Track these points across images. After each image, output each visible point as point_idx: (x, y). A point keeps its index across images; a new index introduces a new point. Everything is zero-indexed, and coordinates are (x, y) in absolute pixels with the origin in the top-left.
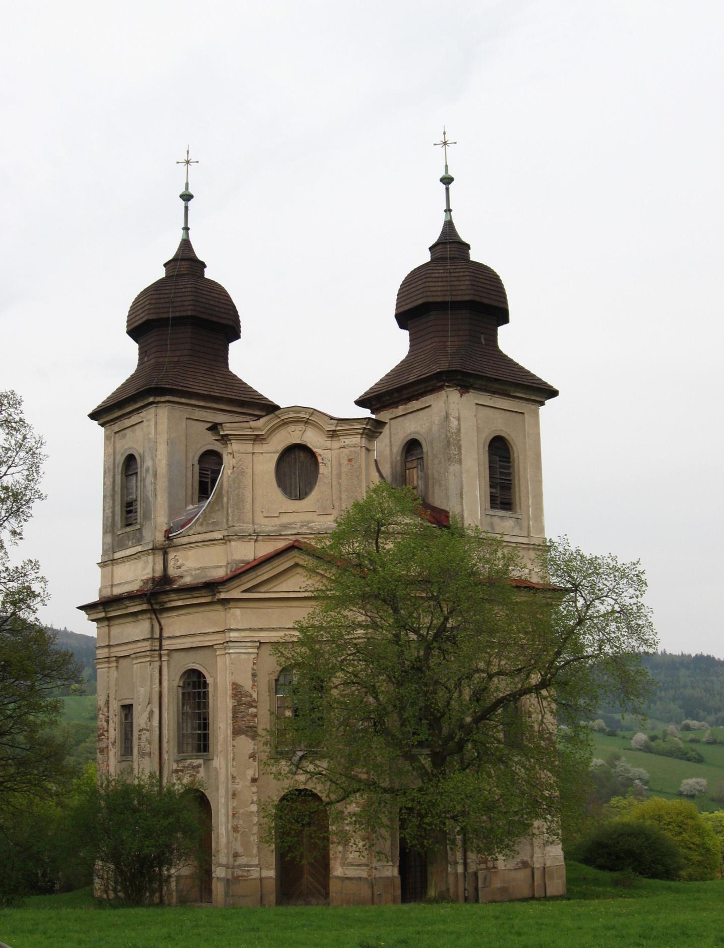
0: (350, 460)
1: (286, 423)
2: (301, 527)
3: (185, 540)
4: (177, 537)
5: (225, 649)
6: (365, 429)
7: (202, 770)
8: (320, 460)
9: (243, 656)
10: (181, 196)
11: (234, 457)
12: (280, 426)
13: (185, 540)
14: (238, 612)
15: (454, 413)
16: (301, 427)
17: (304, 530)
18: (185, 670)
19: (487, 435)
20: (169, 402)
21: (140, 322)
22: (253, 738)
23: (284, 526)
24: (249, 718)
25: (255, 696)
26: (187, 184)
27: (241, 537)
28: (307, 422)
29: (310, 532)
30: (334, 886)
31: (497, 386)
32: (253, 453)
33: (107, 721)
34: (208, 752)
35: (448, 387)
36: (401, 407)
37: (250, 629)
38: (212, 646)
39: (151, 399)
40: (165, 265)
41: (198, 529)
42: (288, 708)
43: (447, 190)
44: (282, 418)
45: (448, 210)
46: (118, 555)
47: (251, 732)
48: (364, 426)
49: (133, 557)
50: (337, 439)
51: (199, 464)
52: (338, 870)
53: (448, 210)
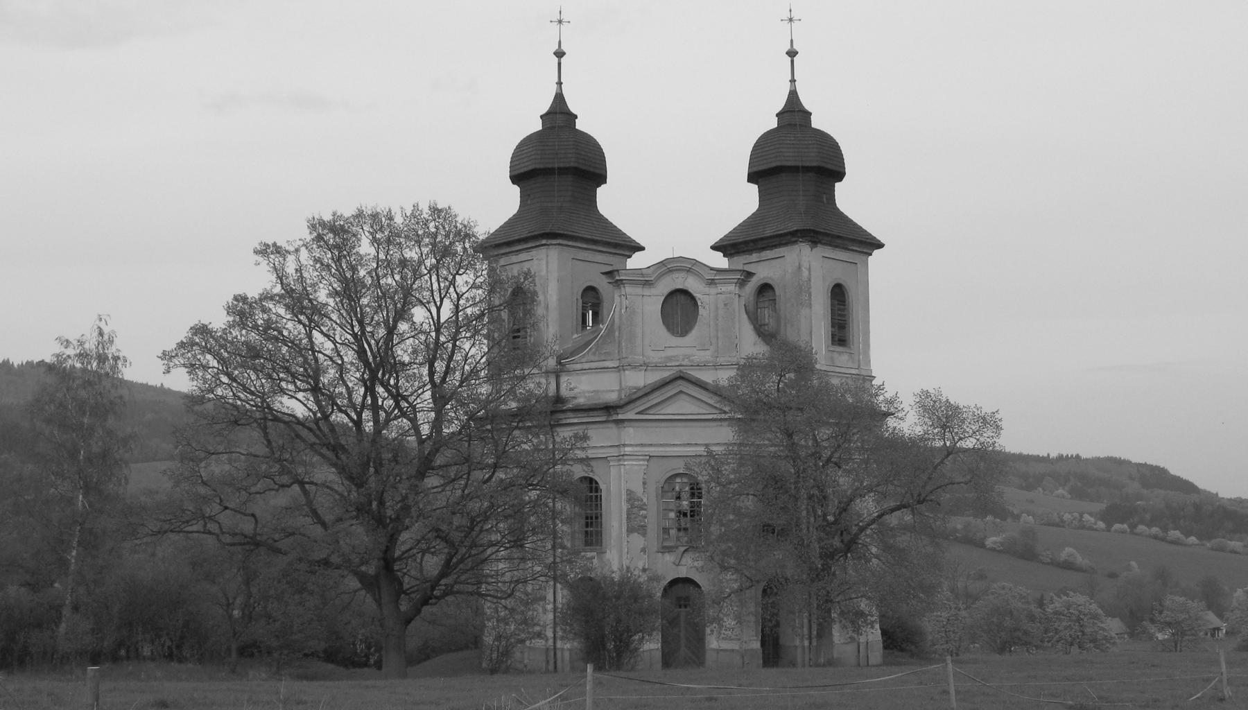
0: (725, 305)
1: (671, 271)
2: (683, 360)
3: (578, 366)
4: (569, 363)
5: (620, 460)
6: (739, 279)
7: (595, 561)
8: (699, 304)
9: (636, 468)
10: (555, 53)
11: (626, 299)
12: (668, 272)
13: (578, 366)
14: (631, 430)
15: (805, 265)
16: (683, 274)
17: (686, 362)
19: (830, 283)
20: (559, 244)
22: (644, 535)
23: (670, 358)
24: (641, 518)
25: (645, 500)
26: (560, 42)
27: (634, 367)
28: (689, 271)
29: (690, 364)
30: (710, 658)
31: (839, 241)
32: (643, 296)
34: (601, 546)
35: (801, 242)
36: (754, 255)
37: (642, 445)
39: (544, 242)
40: (541, 117)
42: (672, 510)
43: (792, 62)
44: (669, 267)
45: (793, 81)
47: (642, 530)
48: (739, 277)
50: (713, 286)
51: (582, 298)
52: (713, 643)
53: (793, 81)
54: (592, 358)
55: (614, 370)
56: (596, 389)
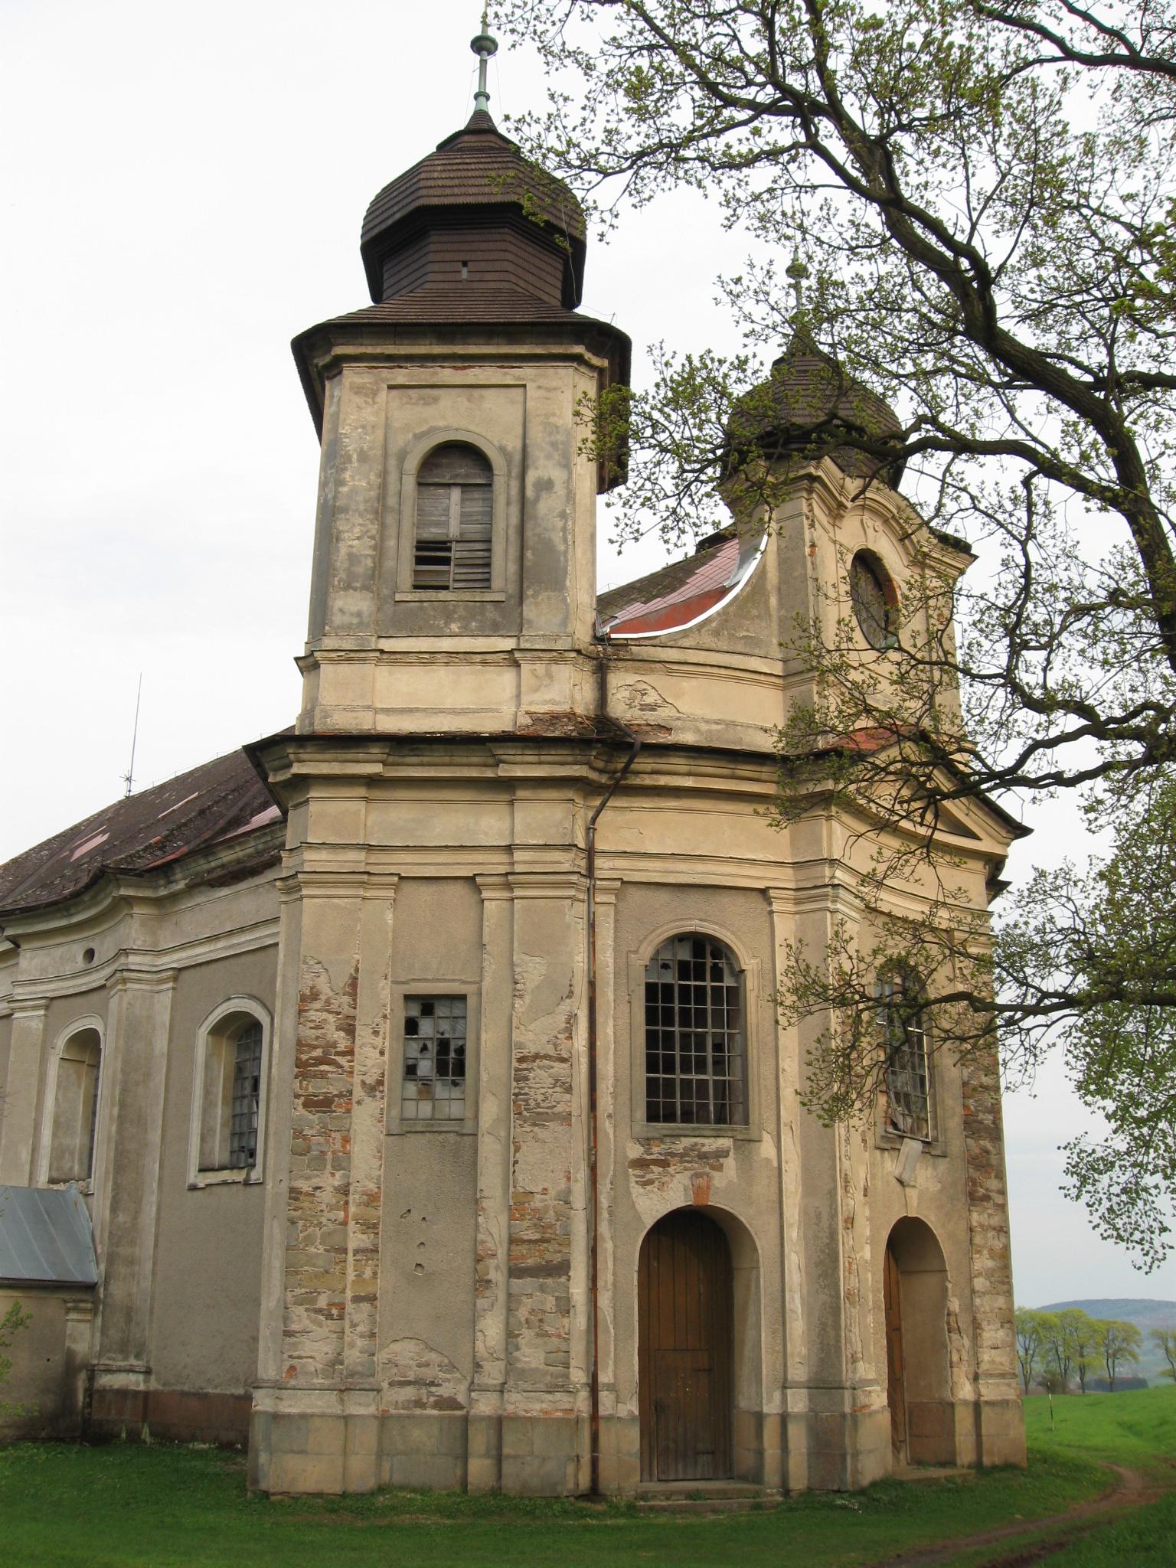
7: (730, 1163)
21: (494, 199)
33: (350, 1030)
34: (746, 1121)
38: (764, 892)
39: (579, 349)
41: (708, 641)
46: (386, 645)
49: (478, 658)
54: (708, 641)
55: (773, 680)
56: (729, 718)
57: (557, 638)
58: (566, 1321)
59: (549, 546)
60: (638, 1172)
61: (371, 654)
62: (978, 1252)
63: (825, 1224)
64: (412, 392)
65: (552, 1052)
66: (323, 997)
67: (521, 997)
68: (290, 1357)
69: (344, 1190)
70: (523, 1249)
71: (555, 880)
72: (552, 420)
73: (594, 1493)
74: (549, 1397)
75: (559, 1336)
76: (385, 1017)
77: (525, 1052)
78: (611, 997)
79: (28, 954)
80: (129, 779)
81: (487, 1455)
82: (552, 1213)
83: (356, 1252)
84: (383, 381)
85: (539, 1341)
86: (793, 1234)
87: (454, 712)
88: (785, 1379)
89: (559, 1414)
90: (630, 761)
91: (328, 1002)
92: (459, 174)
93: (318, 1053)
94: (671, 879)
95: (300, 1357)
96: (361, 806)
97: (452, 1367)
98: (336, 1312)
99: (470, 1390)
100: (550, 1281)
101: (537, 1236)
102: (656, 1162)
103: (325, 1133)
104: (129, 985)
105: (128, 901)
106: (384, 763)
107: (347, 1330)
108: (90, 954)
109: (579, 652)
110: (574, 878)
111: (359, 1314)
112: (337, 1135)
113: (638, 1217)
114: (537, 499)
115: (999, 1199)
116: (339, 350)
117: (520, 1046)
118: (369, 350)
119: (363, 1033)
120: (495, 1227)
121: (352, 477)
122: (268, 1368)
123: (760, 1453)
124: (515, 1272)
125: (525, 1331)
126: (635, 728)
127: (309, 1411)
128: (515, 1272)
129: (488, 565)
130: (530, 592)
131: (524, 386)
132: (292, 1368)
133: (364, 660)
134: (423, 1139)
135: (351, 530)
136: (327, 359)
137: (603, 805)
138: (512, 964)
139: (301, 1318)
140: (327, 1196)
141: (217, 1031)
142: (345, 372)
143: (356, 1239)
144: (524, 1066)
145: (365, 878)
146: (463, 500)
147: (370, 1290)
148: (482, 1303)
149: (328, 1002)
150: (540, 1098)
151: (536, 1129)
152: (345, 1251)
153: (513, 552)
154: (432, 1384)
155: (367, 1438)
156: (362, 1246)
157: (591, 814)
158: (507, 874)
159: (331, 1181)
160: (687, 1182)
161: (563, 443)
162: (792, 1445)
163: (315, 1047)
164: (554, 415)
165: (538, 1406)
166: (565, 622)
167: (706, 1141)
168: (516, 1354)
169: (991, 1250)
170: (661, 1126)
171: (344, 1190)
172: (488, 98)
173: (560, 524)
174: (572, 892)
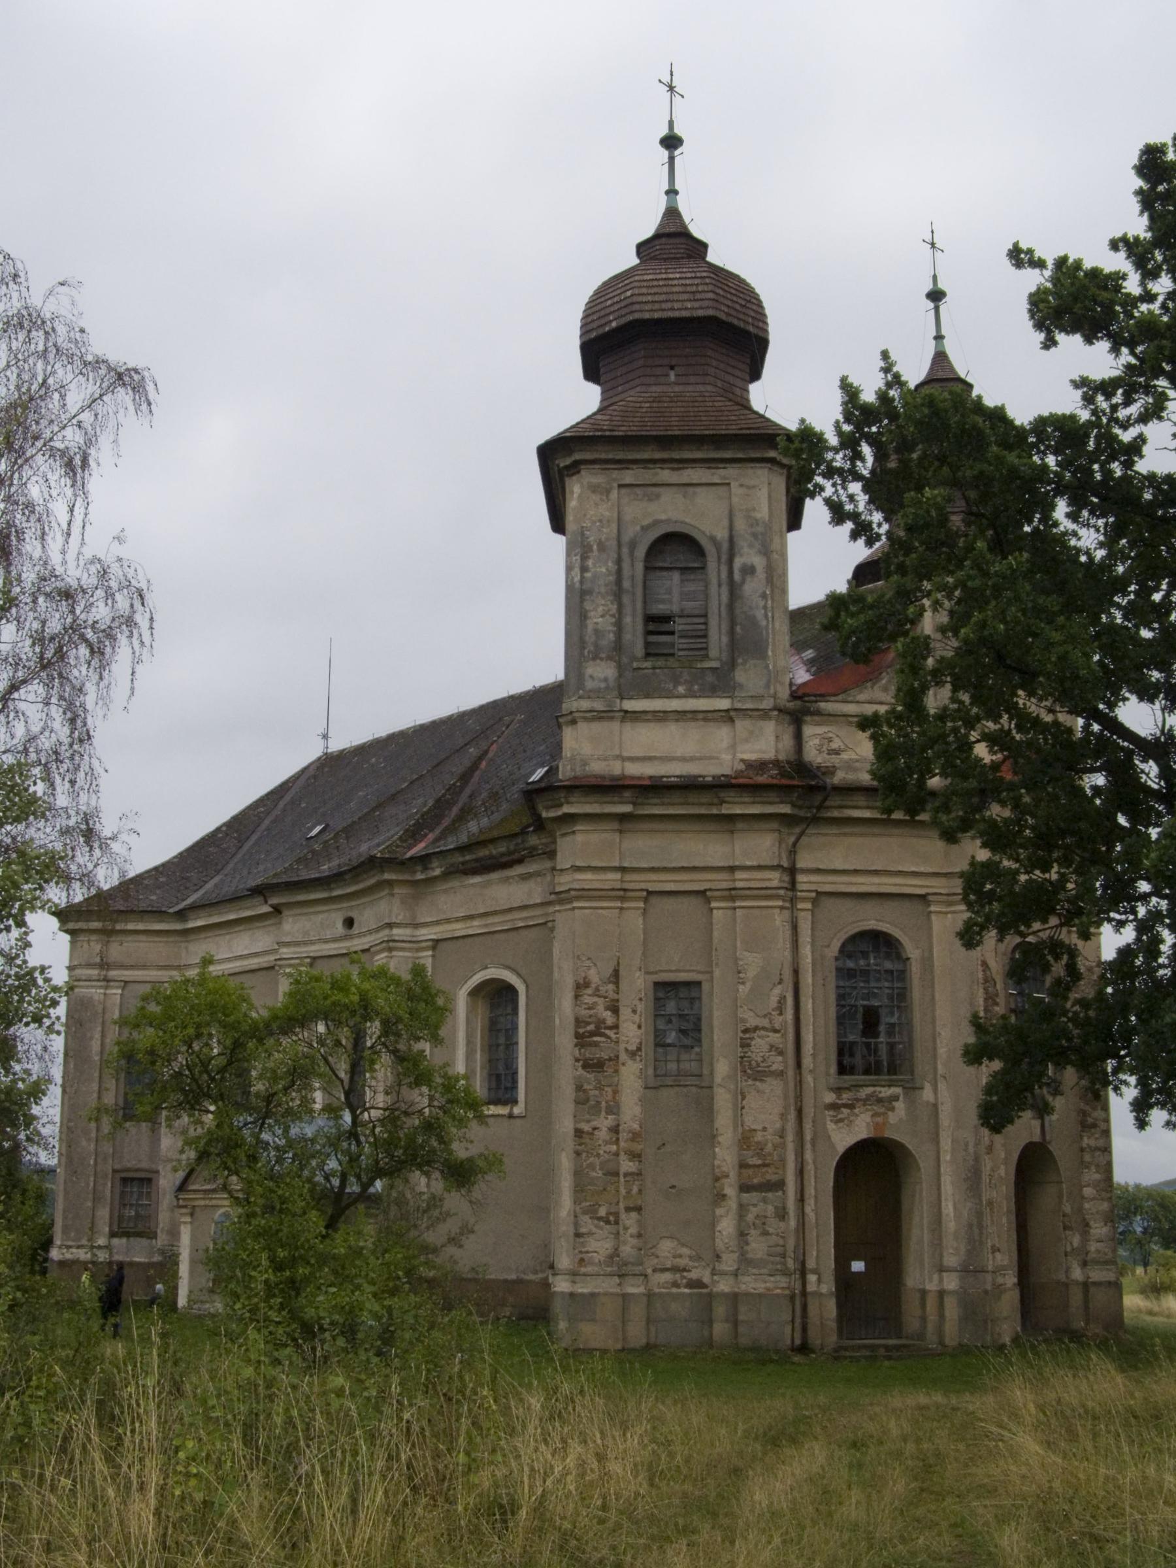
7: (900, 1105)
18: (847, 935)
33: (615, 1010)
38: (923, 897)
46: (630, 705)
49: (701, 716)
53: (939, 337)
57: (760, 698)
58: (782, 1224)
59: (753, 621)
60: (831, 1113)
61: (617, 714)
62: (1087, 1167)
63: (971, 1149)
64: (638, 491)
65: (767, 1025)
66: (594, 986)
67: (743, 983)
68: (581, 1252)
69: (615, 1130)
70: (750, 1171)
71: (765, 893)
72: (753, 514)
73: (804, 1348)
74: (772, 1279)
75: (777, 1235)
76: (641, 999)
77: (748, 1025)
78: (810, 981)
79: (290, 920)
80: (325, 737)
81: (727, 1321)
82: (770, 1145)
83: (626, 1175)
84: (614, 480)
85: (762, 1239)
86: (946, 1157)
87: (684, 759)
88: (941, 1265)
89: (779, 1291)
90: (825, 799)
91: (597, 989)
92: (665, 290)
93: (591, 1027)
94: (854, 889)
95: (587, 1252)
96: (617, 836)
97: (699, 1258)
98: (613, 1220)
99: (713, 1274)
100: (770, 1195)
101: (760, 1162)
102: (846, 1106)
103: (600, 1088)
104: (394, 953)
105: (390, 883)
106: (634, 804)
107: (622, 1232)
108: (349, 923)
109: (780, 710)
110: (782, 892)
111: (630, 1221)
112: (609, 1090)
113: (832, 1146)
114: (743, 582)
115: (1103, 1126)
116: (577, 456)
117: (743, 1020)
118: (603, 456)
119: (625, 1012)
120: (726, 1156)
121: (594, 564)
122: (564, 1262)
123: (924, 1319)
124: (745, 1188)
125: (753, 1232)
126: (823, 770)
127: (596, 1291)
128: (745, 1188)
129: (705, 636)
130: (740, 661)
131: (729, 484)
132: (582, 1260)
133: (612, 718)
134: (672, 1091)
135: (595, 610)
136: (568, 461)
137: (802, 834)
138: (736, 959)
139: (587, 1225)
140: (603, 1134)
141: (475, 993)
142: (583, 473)
143: (627, 1165)
144: (747, 1036)
145: (622, 894)
146: (682, 581)
147: (639, 1202)
148: (719, 1211)
149: (597, 989)
150: (760, 1059)
151: (758, 1083)
152: (617, 1174)
153: (725, 627)
154: (684, 1270)
155: (638, 1312)
156: (630, 1170)
157: (792, 839)
158: (730, 889)
159: (605, 1122)
160: (869, 1120)
161: (762, 534)
162: (947, 1314)
163: (588, 1023)
164: (754, 509)
165: (763, 1286)
166: (768, 686)
167: (883, 1089)
168: (746, 1248)
169: (1097, 1166)
170: (849, 1079)
171: (615, 1130)
172: (676, 193)
173: (762, 603)
174: (780, 903)
